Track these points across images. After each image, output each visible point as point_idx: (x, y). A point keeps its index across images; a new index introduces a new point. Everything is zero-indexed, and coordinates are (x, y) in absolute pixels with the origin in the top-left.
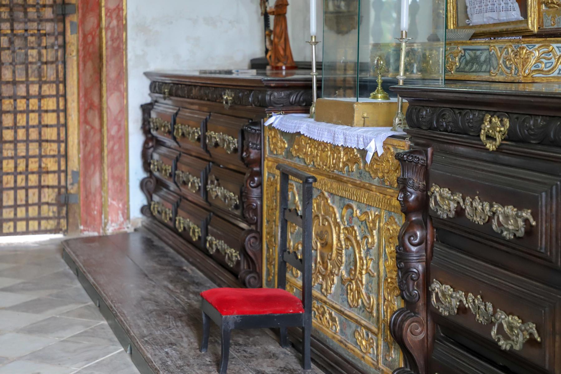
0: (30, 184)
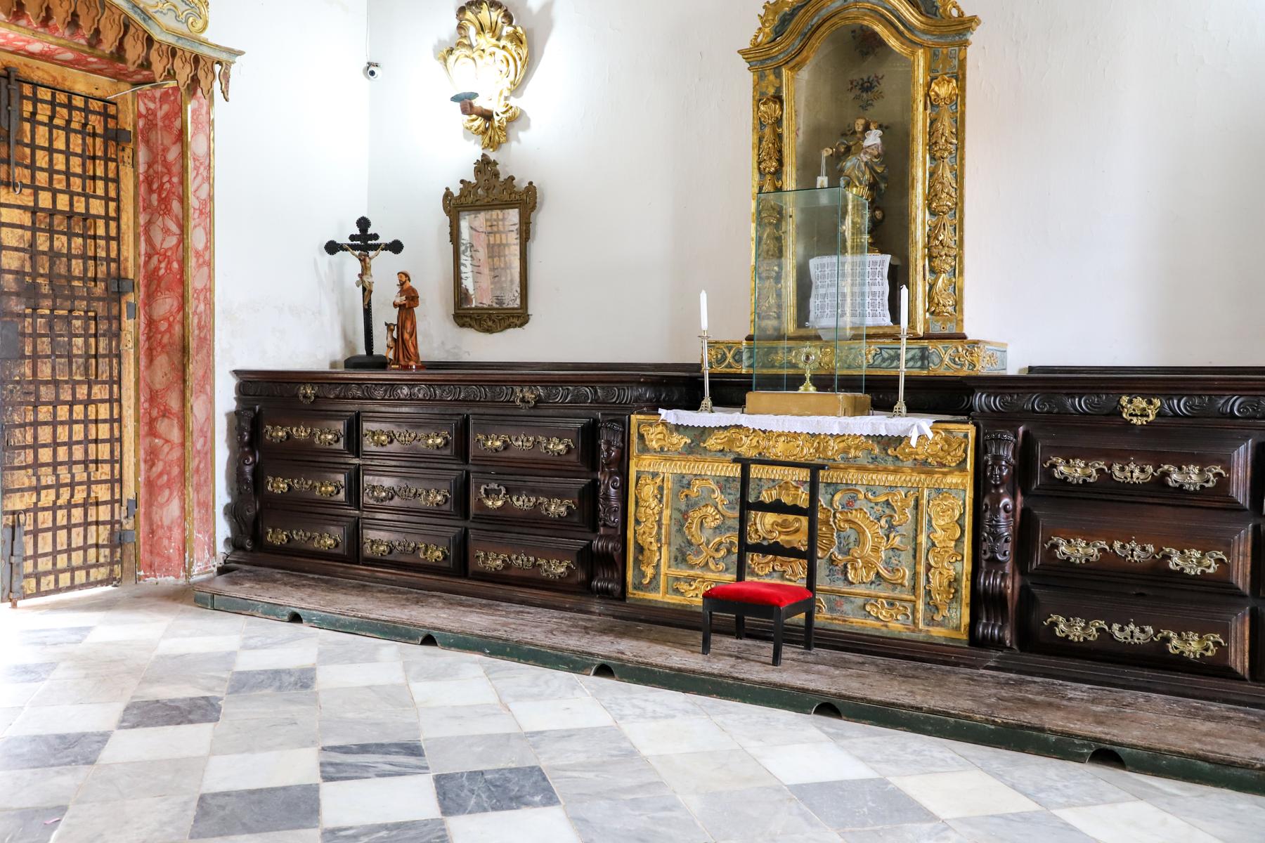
0: (73, 521)
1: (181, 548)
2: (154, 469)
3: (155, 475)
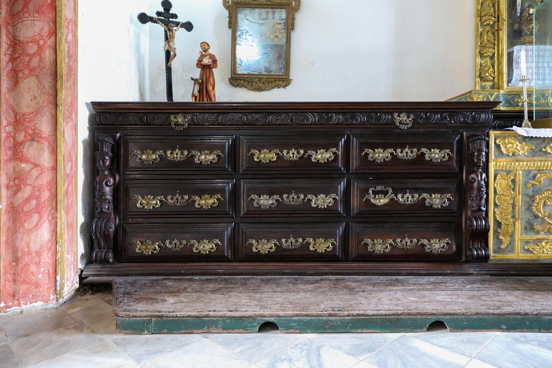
1: (51, 272)
2: (19, 195)
3: (21, 201)
